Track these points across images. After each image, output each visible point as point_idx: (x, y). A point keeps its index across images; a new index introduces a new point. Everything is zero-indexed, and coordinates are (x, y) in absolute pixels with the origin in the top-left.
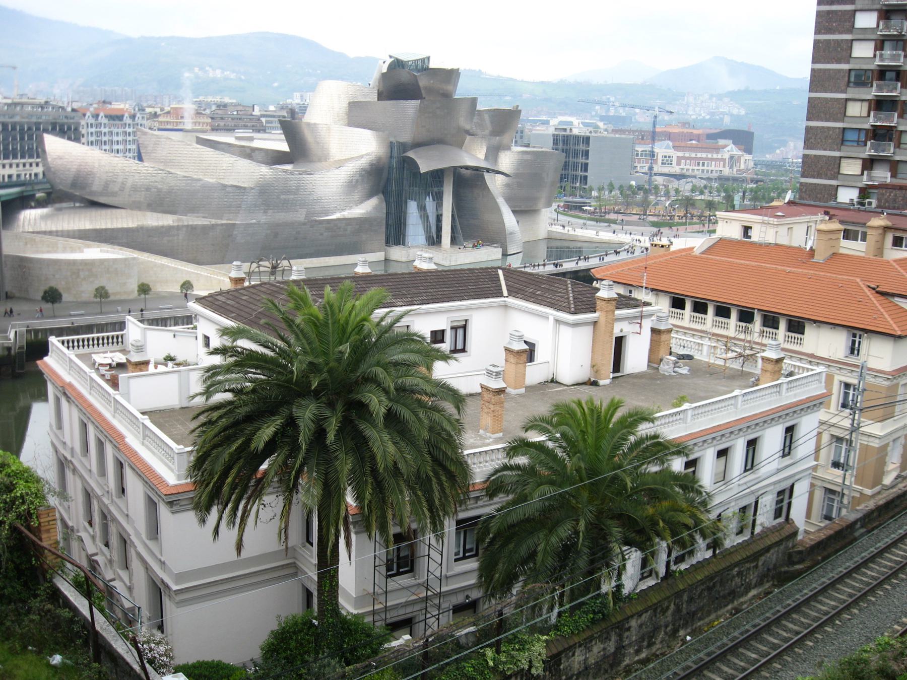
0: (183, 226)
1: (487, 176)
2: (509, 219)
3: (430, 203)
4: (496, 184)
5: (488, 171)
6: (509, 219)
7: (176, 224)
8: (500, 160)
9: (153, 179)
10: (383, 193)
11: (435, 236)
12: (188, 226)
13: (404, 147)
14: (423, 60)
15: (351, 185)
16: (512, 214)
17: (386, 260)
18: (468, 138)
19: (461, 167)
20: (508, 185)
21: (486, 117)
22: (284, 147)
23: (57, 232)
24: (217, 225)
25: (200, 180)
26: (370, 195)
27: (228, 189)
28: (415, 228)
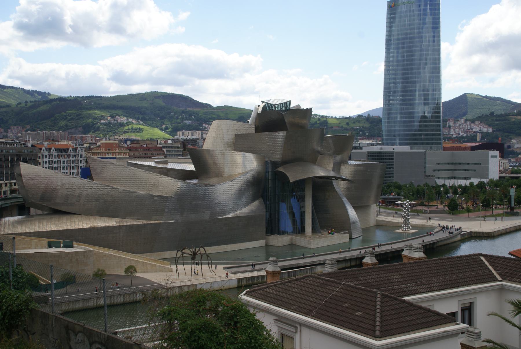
0: (123, 226)
1: (335, 183)
2: (352, 213)
3: (293, 202)
4: (340, 186)
5: (337, 178)
6: (352, 213)
7: (118, 225)
8: (341, 171)
9: (101, 193)
10: (262, 197)
11: (300, 226)
12: (126, 226)
13: (275, 164)
14: (286, 103)
15: (240, 193)
16: (353, 209)
17: (267, 245)
18: (320, 156)
19: (317, 177)
20: (348, 189)
21: (330, 141)
22: (191, 167)
23: (30, 233)
24: (147, 224)
25: (135, 192)
26: (253, 200)
27: (156, 198)
28: (286, 223)
